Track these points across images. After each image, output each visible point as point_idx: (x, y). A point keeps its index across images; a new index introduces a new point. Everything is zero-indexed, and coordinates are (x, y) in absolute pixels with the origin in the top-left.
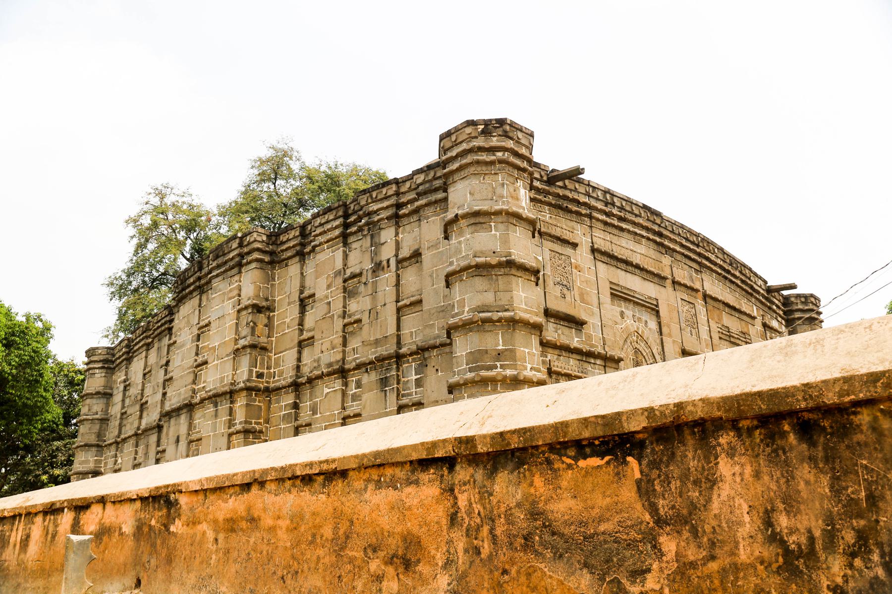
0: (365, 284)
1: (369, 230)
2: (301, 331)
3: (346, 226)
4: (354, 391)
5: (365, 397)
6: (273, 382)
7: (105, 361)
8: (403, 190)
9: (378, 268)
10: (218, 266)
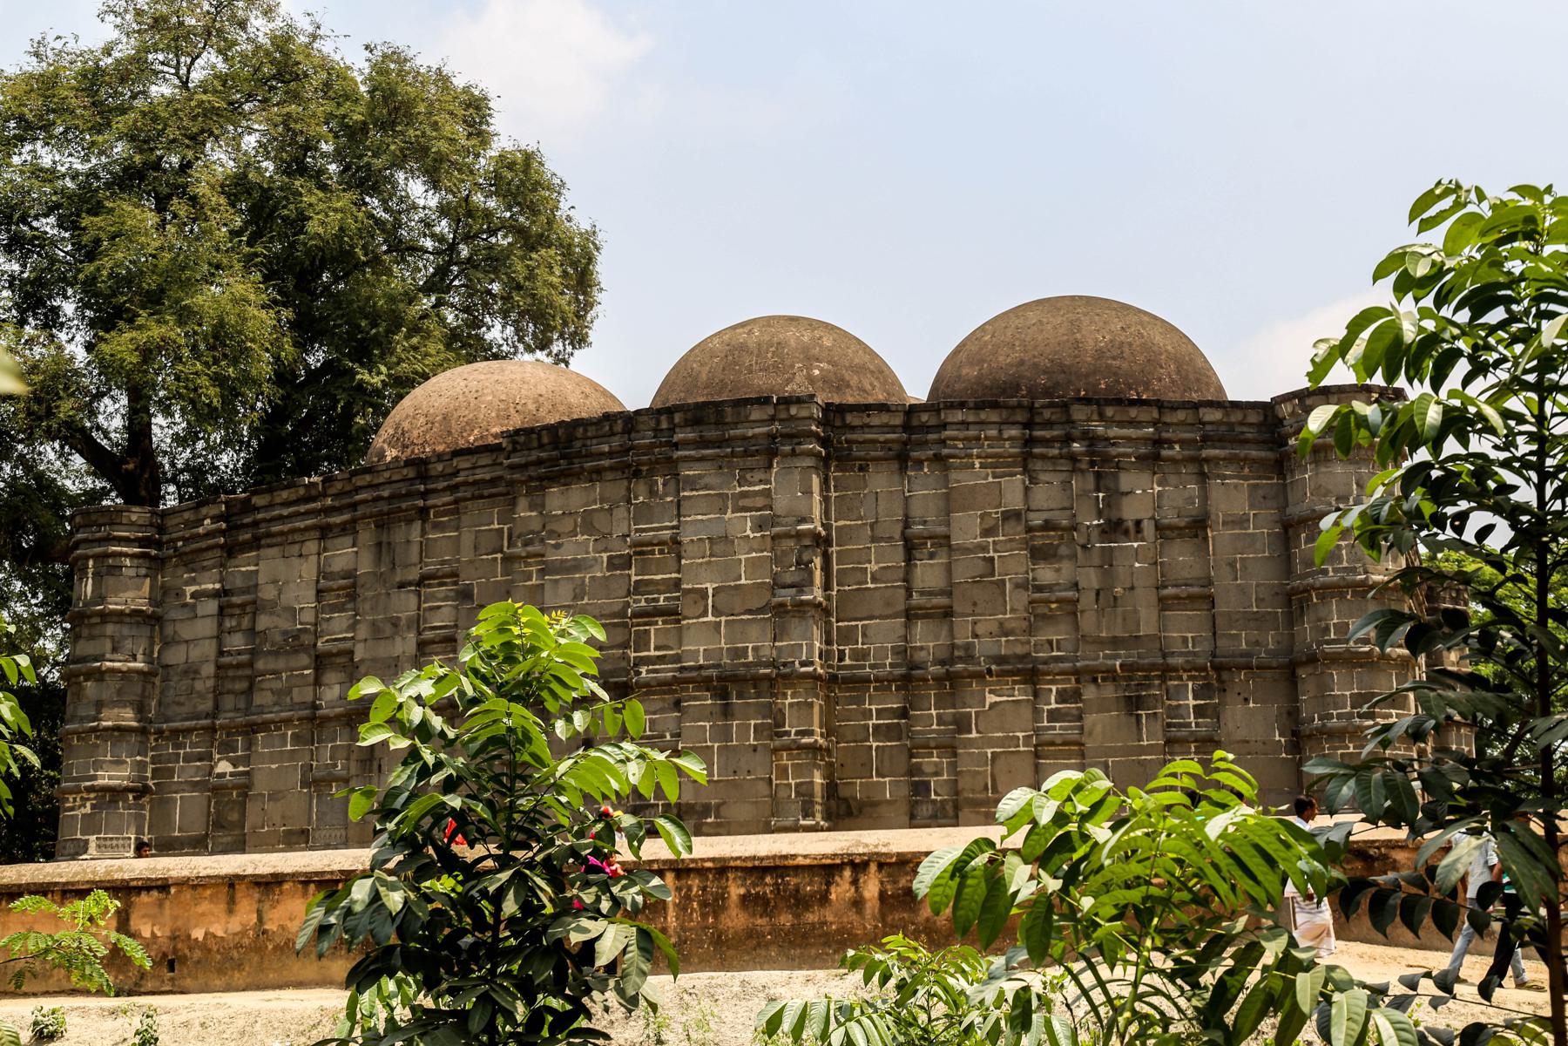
0: (1084, 547)
1: (1092, 464)
2: (909, 592)
3: (1029, 442)
4: (1054, 706)
5: (1090, 719)
6: (840, 668)
7: (141, 542)
8: (1168, 418)
9: (1115, 528)
10: (702, 443)
